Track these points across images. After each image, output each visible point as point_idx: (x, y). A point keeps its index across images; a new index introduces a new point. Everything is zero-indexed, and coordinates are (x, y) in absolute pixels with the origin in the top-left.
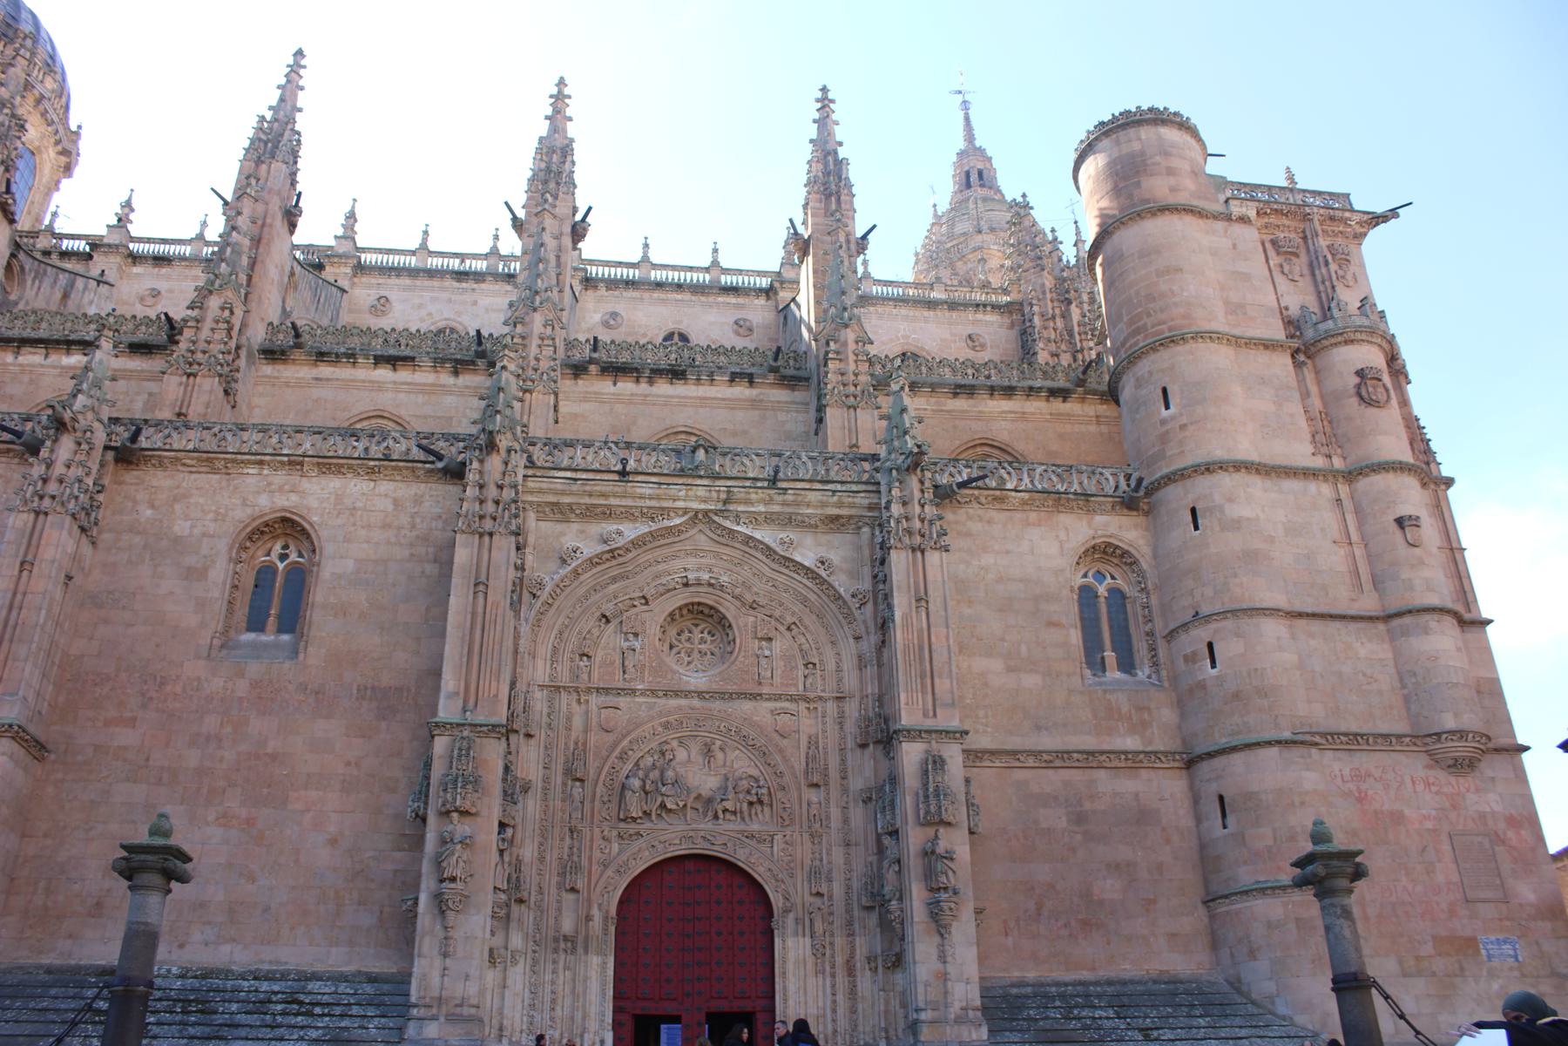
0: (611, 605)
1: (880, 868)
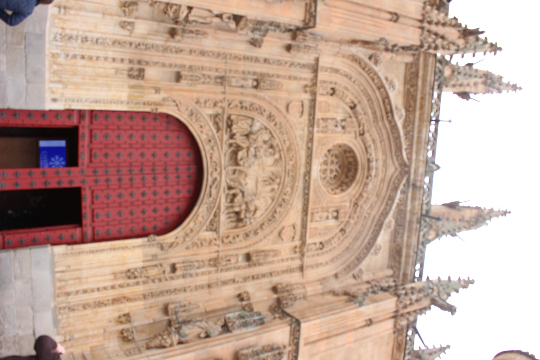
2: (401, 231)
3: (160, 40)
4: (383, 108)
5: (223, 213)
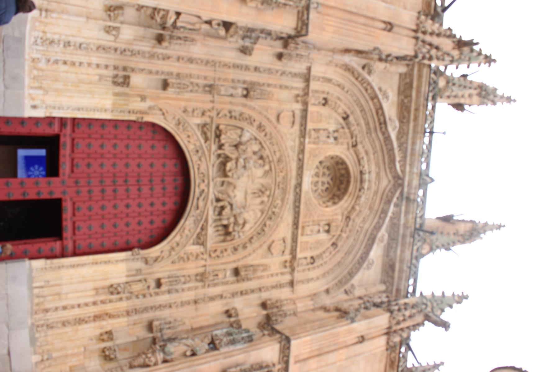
2: (394, 245)
3: (146, 47)
5: (211, 226)
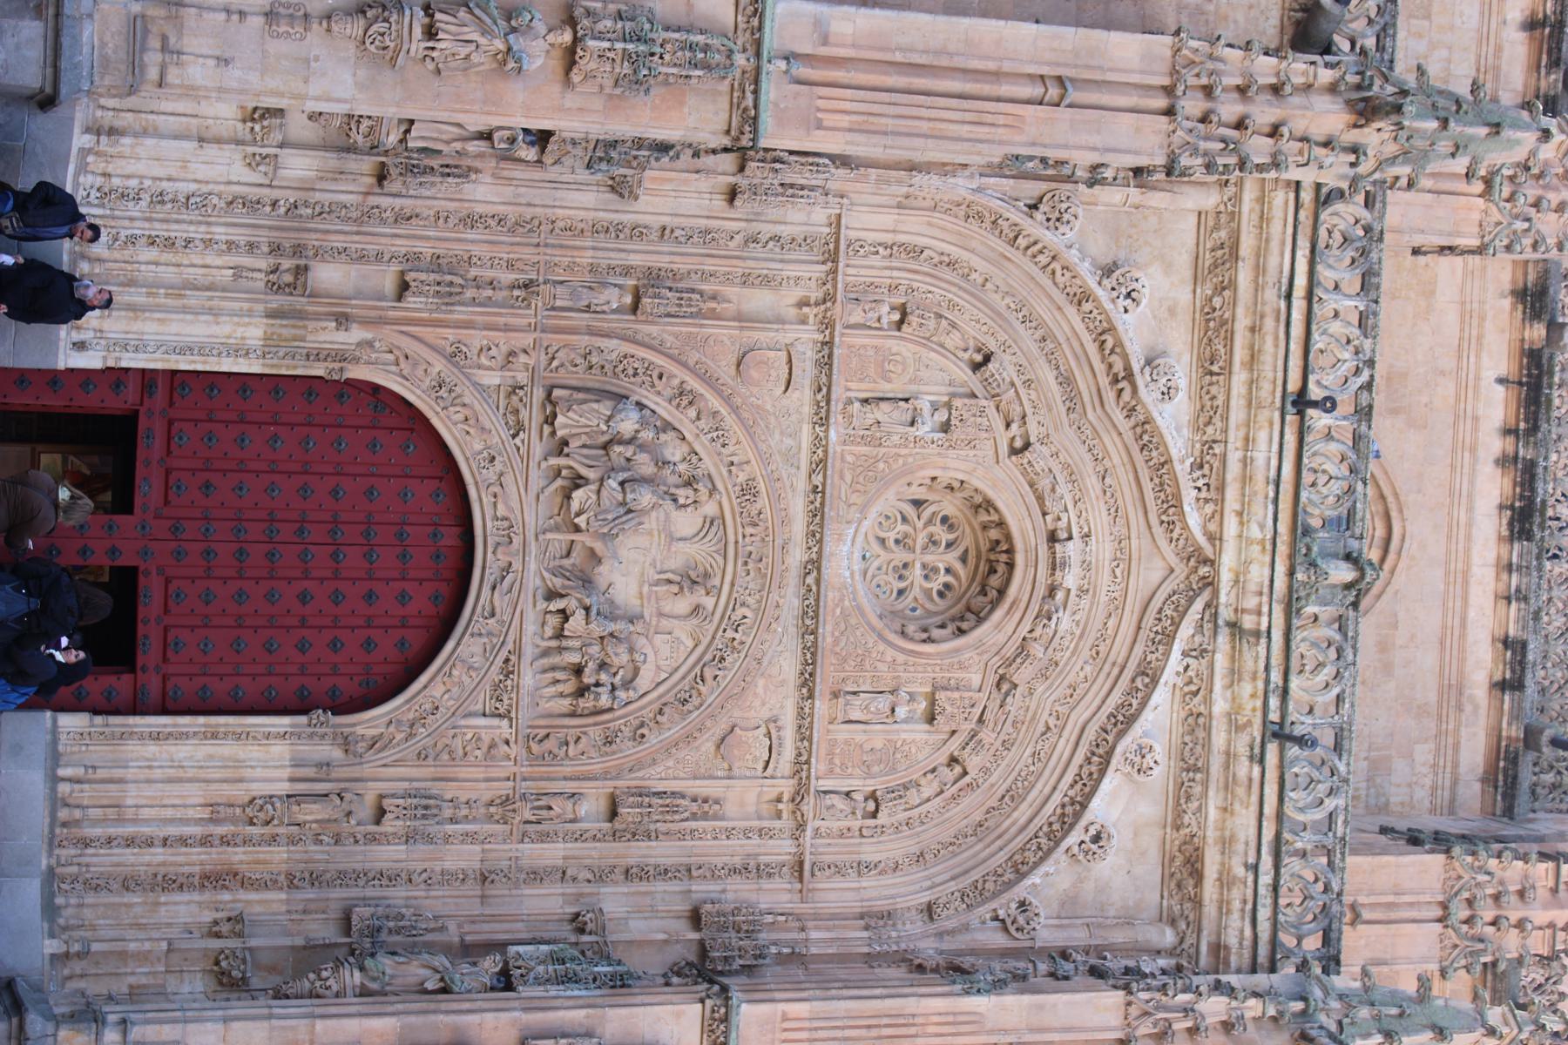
0: (1010, 373)
1: (431, 948)
4: (1100, 367)
